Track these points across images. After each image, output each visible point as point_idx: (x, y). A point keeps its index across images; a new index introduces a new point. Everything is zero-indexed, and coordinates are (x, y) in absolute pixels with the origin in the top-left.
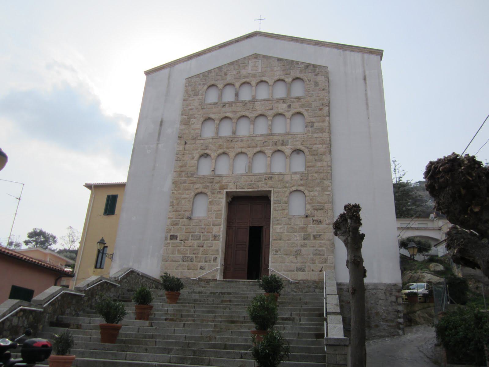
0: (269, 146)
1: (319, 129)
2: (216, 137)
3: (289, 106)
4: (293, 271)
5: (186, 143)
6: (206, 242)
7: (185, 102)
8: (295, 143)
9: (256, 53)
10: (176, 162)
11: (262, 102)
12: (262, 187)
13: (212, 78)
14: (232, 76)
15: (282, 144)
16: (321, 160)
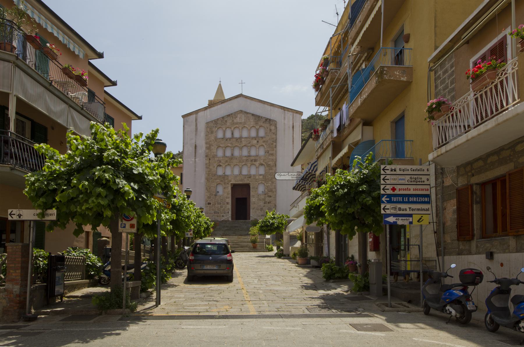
3: (258, 142)
5: (210, 159)
15: (255, 161)
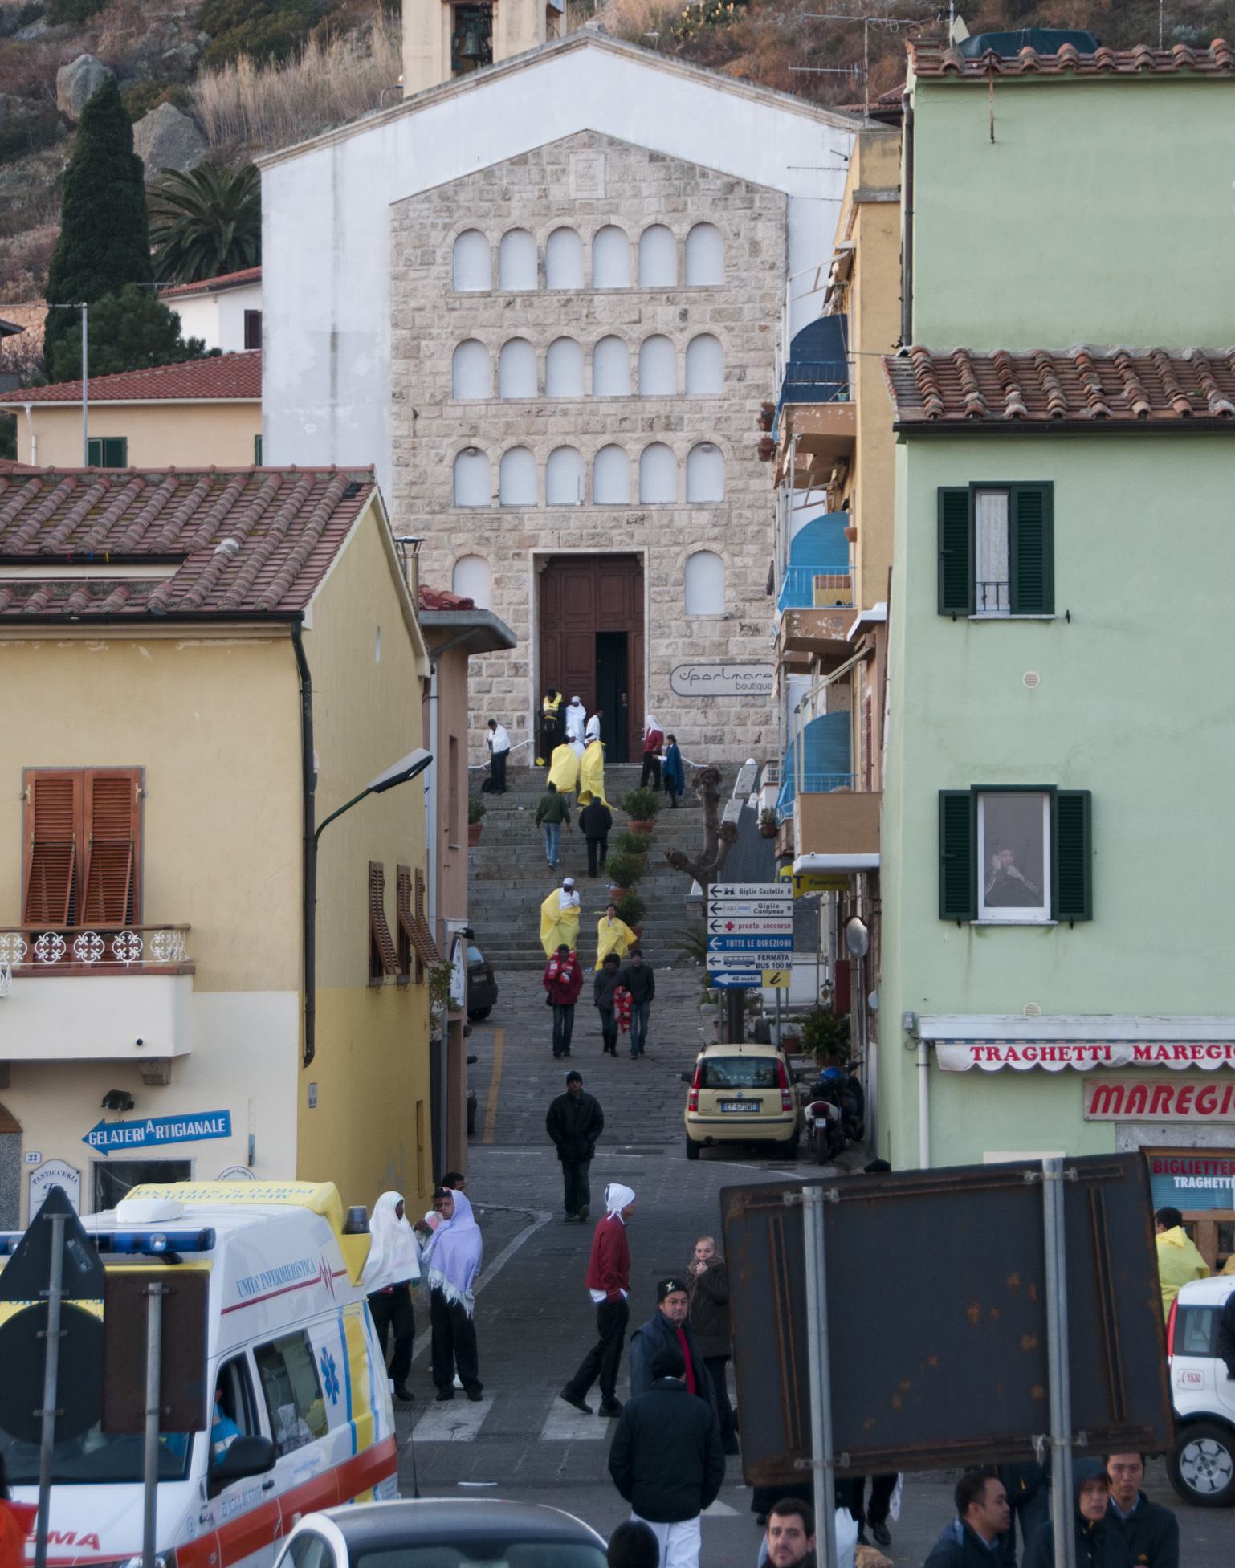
0: (633, 431)
1: (758, 386)
2: (495, 402)
3: (684, 315)
4: (698, 743)
5: (416, 416)
6: (495, 680)
7: (398, 283)
8: (698, 426)
9: (589, 127)
10: (398, 469)
11: (611, 297)
12: (621, 542)
13: (469, 209)
14: (525, 206)
15: (668, 427)
16: (761, 475)
